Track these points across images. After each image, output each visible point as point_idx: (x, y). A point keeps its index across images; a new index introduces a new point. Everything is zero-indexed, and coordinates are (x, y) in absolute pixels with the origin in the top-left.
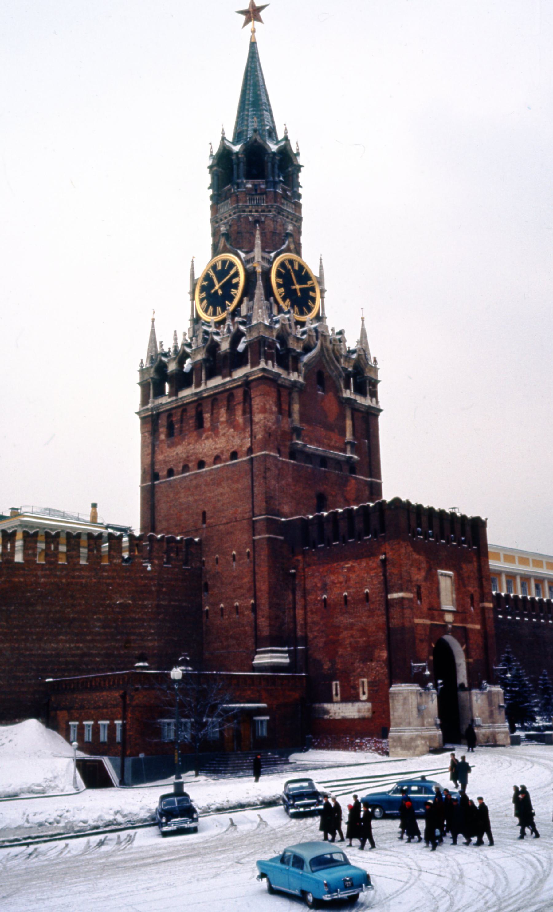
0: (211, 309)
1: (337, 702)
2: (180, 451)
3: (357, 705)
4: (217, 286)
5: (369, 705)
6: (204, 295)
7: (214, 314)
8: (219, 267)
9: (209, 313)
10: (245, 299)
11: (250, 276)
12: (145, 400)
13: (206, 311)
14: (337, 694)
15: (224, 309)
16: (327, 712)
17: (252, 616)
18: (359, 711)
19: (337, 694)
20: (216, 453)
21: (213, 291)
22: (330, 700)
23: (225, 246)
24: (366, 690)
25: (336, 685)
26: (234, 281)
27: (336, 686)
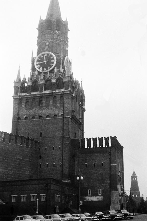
0: (41, 68)
1: (89, 196)
2: (32, 112)
3: (97, 197)
4: (45, 61)
8: (46, 55)
9: (40, 69)
10: (56, 68)
12: (16, 93)
13: (39, 68)
14: (89, 194)
15: (47, 69)
16: (86, 199)
17: (61, 168)
18: (98, 199)
19: (89, 194)
20: (47, 114)
22: (87, 196)
23: (47, 49)
24: (101, 192)
25: (89, 191)
26: (52, 61)
27: (89, 191)
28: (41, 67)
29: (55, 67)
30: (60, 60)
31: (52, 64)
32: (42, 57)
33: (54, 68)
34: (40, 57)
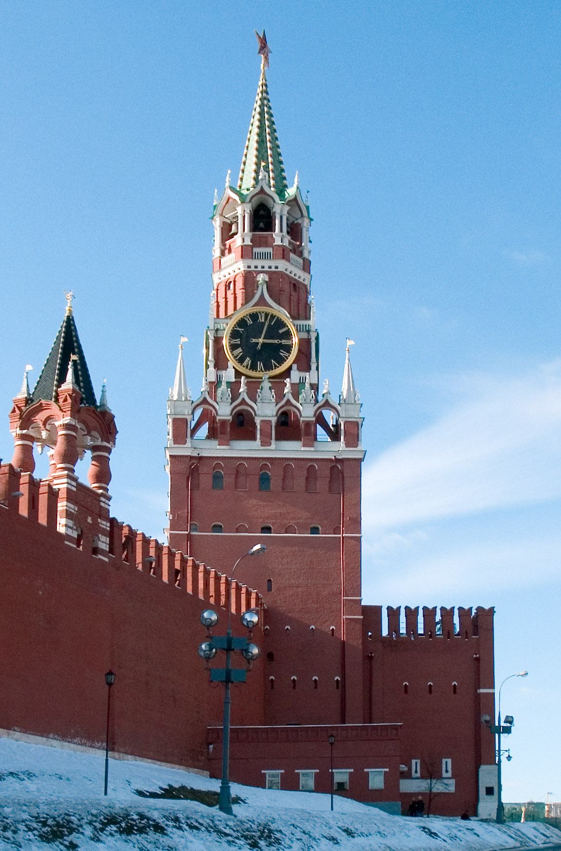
0: (248, 361)
1: (417, 778)
4: (261, 340)
5: (453, 781)
6: (238, 341)
7: (253, 367)
9: (245, 364)
11: (305, 344)
13: (241, 360)
14: (416, 772)
19: (416, 772)
21: (254, 340)
24: (449, 768)
28: (248, 359)
29: (294, 362)
30: (308, 341)
31: (283, 353)
32: (250, 322)
33: (290, 368)
34: (242, 323)
